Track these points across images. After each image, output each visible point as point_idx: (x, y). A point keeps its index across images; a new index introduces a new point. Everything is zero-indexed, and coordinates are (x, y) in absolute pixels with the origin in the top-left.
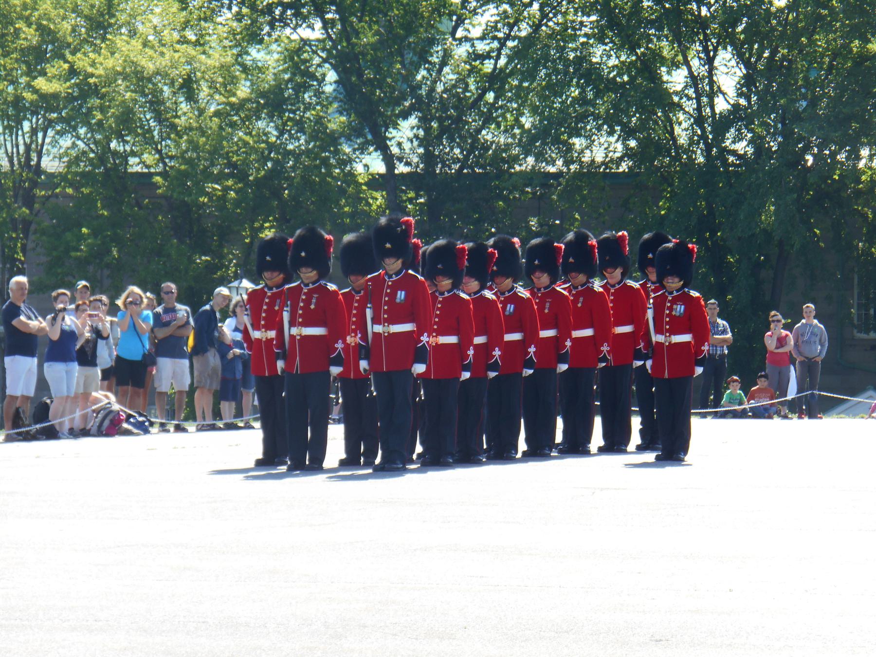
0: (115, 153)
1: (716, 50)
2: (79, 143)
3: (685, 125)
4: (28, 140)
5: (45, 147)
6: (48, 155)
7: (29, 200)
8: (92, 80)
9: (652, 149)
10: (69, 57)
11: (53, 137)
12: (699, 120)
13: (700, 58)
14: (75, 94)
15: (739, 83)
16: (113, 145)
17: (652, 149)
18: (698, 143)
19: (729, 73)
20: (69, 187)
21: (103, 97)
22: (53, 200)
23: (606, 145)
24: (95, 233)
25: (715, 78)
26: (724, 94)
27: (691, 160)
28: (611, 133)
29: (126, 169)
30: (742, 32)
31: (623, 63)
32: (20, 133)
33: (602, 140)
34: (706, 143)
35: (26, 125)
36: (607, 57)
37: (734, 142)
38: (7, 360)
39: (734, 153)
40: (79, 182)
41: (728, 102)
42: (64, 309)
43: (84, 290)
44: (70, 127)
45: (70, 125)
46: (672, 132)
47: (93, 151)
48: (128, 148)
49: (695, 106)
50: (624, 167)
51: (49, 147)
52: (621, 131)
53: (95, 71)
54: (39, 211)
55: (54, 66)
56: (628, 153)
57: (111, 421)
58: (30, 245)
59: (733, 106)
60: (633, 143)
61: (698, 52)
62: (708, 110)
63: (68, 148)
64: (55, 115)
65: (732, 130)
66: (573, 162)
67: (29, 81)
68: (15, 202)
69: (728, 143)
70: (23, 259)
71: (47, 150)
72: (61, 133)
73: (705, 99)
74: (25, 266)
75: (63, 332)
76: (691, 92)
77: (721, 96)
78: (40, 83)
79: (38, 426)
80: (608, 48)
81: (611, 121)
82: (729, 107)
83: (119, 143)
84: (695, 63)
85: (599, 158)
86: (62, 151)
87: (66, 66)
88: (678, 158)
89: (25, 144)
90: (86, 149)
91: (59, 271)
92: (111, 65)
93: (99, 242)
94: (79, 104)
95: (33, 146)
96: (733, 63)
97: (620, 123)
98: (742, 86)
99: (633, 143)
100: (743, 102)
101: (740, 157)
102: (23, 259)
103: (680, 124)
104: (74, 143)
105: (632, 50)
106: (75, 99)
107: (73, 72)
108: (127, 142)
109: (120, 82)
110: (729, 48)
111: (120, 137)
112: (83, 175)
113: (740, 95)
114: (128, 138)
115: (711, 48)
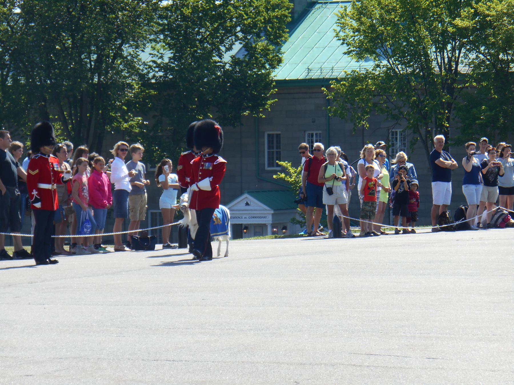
0: (503, 60)
2: (481, 55)
4: (450, 55)
5: (460, 59)
6: (462, 62)
7: (451, 91)
8: (488, 19)
10: (475, 6)
11: (465, 53)
14: (478, 27)
16: (500, 57)
20: (474, 82)
21: (495, 27)
22: (464, 89)
24: (490, 108)
29: (508, 70)
32: (445, 51)
35: (449, 47)
38: (433, 184)
40: (480, 78)
42: (475, 153)
43: (484, 143)
44: (474, 45)
45: (475, 46)
47: (488, 60)
48: (510, 58)
51: (463, 59)
53: (490, 13)
54: (457, 97)
55: (465, 11)
57: (503, 219)
58: (451, 117)
63: (474, 59)
64: (466, 40)
67: (451, 21)
68: (443, 92)
70: (448, 125)
71: (462, 60)
72: (469, 51)
74: (449, 129)
75: (474, 167)
78: (458, 22)
79: (457, 223)
83: (504, 55)
86: (470, 61)
87: (473, 11)
89: (448, 57)
90: (485, 59)
91: (470, 131)
92: (500, 9)
93: (493, 114)
94: (481, 32)
95: (453, 58)
102: (448, 125)
104: (477, 56)
106: (478, 30)
107: (476, 14)
108: (509, 54)
109: (505, 18)
111: (505, 51)
112: (483, 74)
114: (510, 52)
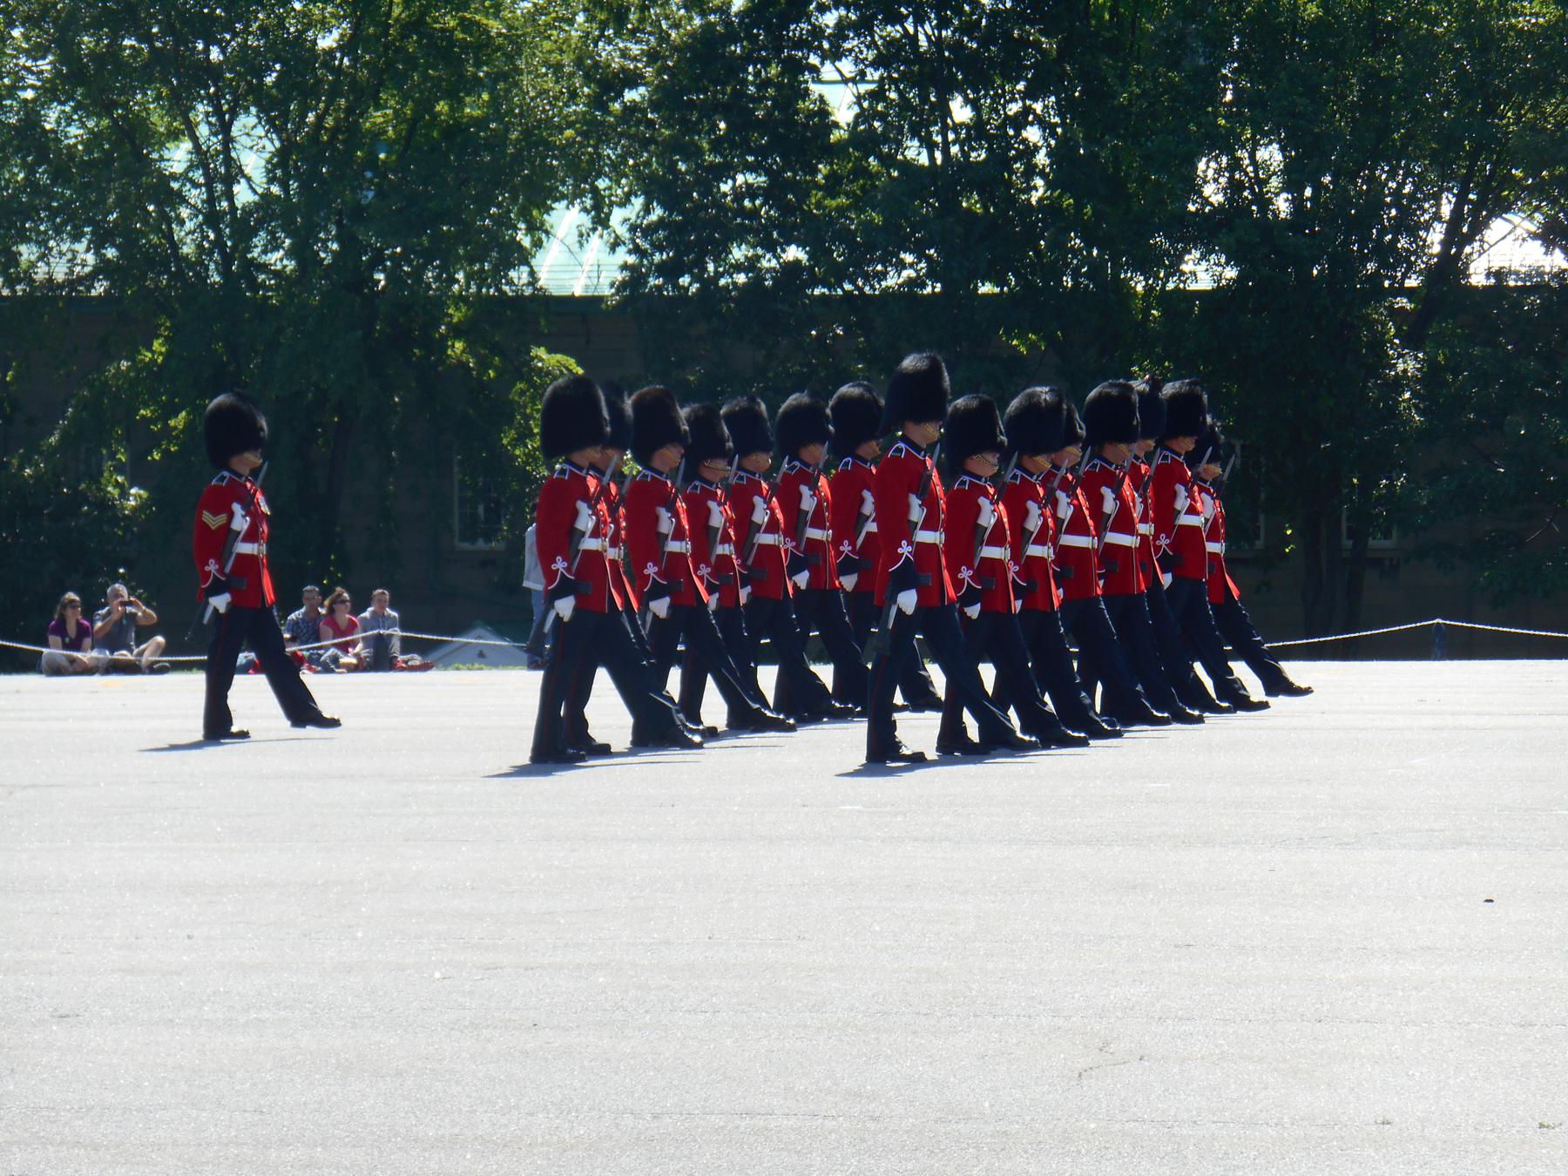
1: (234, 115)
3: (189, 225)
9: (142, 262)
12: (212, 218)
13: (209, 123)
15: (269, 162)
17: (142, 262)
18: (210, 253)
19: (254, 149)
23: (69, 256)
25: (233, 154)
26: (249, 179)
27: (202, 278)
28: (76, 238)
30: (276, 84)
31: (91, 132)
33: (64, 247)
34: (222, 253)
36: (67, 125)
37: (265, 252)
39: (264, 268)
41: (255, 192)
46: (169, 235)
49: (205, 197)
50: (99, 288)
52: (93, 233)
56: (103, 268)
59: (262, 196)
60: (111, 253)
61: (207, 114)
62: (225, 204)
65: (262, 234)
66: (19, 281)
69: (255, 253)
73: (219, 187)
76: (198, 175)
77: (243, 181)
80: (67, 109)
81: (71, 222)
82: (256, 198)
84: (203, 131)
85: (60, 274)
88: (180, 275)
96: (260, 131)
97: (89, 222)
98: (275, 166)
99: (111, 253)
100: (275, 189)
101: (277, 274)
103: (182, 223)
105: (106, 108)
110: (253, 110)
113: (271, 181)
115: (225, 107)
